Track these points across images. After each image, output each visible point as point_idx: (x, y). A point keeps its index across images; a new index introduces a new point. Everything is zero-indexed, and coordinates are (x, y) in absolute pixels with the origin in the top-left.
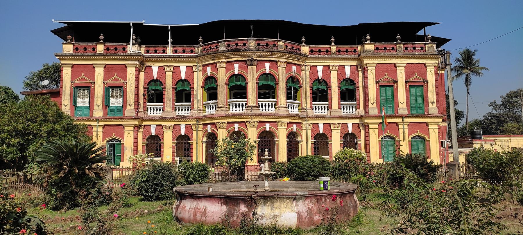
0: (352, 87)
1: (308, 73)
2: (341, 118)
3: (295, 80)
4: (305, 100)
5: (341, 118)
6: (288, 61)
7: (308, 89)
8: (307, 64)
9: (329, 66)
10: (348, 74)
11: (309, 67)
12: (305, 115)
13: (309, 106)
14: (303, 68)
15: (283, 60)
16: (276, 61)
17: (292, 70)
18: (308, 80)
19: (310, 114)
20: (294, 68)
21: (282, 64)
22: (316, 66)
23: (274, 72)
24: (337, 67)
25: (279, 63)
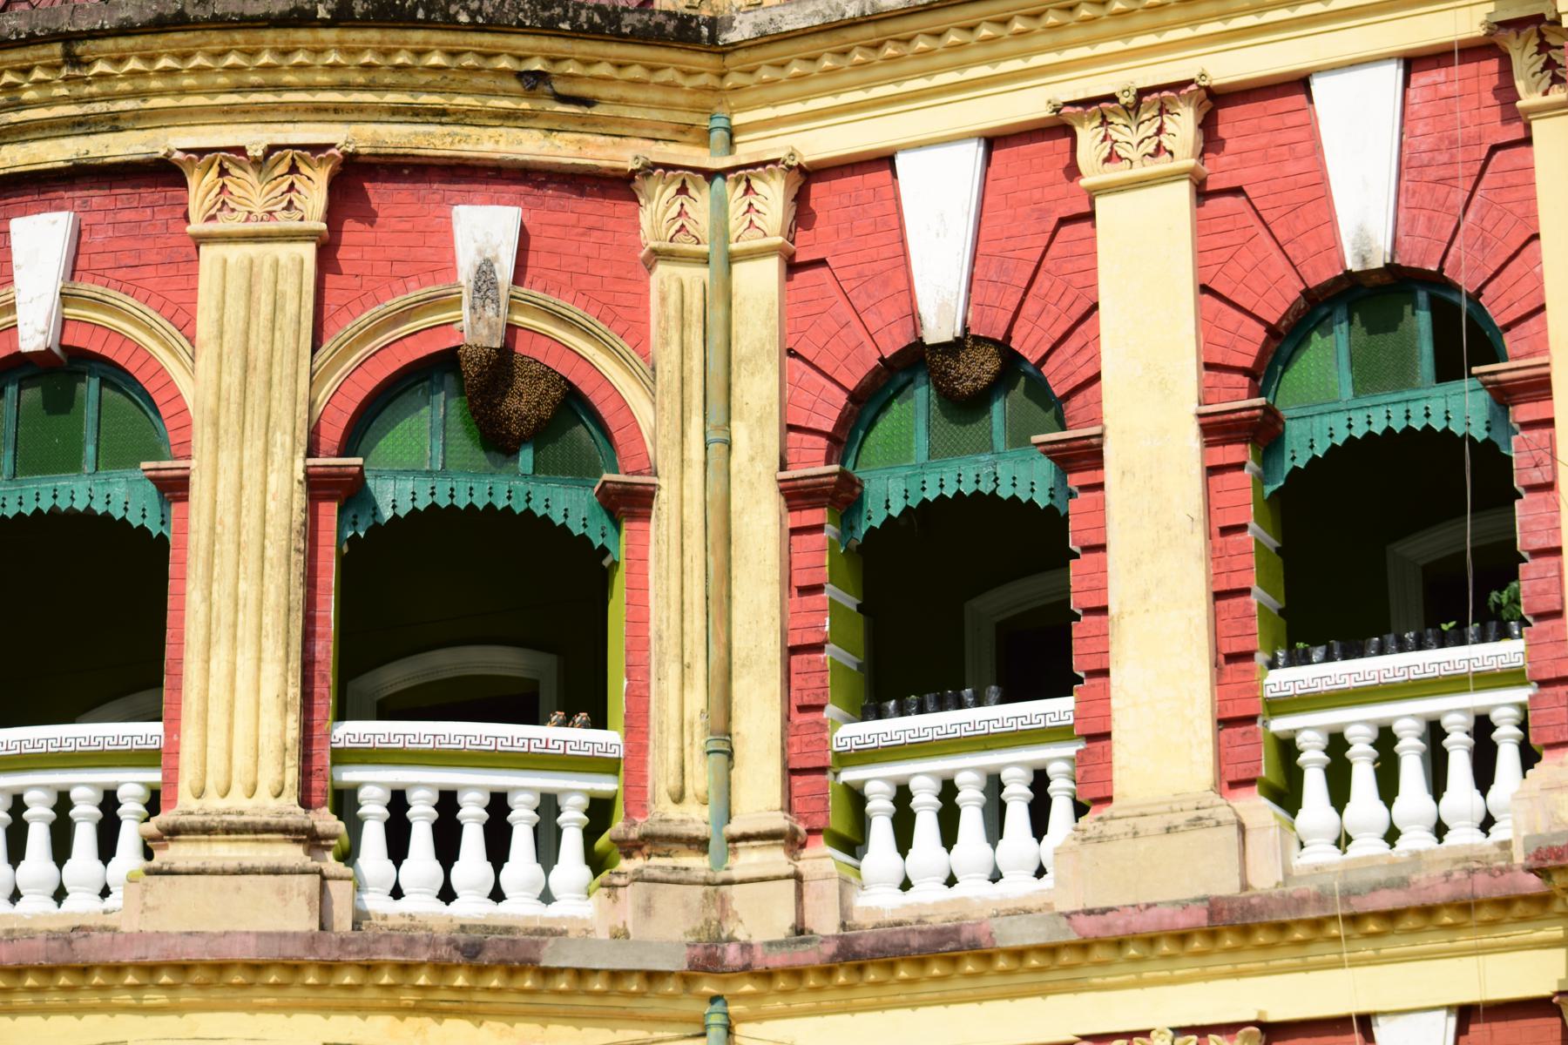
0: (1461, 408)
1: (759, 282)
2: (1238, 927)
3: (522, 402)
4: (696, 699)
5: (1238, 927)
6: (342, 136)
7: (760, 519)
8: (747, 151)
9: (1057, 128)
10: (1365, 221)
11: (773, 196)
12: (665, 926)
13: (759, 797)
14: (656, 213)
15: (255, 137)
16: (164, 174)
17: (445, 265)
18: (759, 389)
19: (761, 918)
20: (484, 230)
21: (253, 194)
22: (885, 161)
23: (130, 326)
24: (1183, 126)
25: (201, 187)
